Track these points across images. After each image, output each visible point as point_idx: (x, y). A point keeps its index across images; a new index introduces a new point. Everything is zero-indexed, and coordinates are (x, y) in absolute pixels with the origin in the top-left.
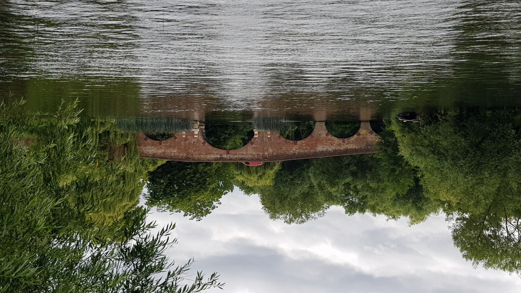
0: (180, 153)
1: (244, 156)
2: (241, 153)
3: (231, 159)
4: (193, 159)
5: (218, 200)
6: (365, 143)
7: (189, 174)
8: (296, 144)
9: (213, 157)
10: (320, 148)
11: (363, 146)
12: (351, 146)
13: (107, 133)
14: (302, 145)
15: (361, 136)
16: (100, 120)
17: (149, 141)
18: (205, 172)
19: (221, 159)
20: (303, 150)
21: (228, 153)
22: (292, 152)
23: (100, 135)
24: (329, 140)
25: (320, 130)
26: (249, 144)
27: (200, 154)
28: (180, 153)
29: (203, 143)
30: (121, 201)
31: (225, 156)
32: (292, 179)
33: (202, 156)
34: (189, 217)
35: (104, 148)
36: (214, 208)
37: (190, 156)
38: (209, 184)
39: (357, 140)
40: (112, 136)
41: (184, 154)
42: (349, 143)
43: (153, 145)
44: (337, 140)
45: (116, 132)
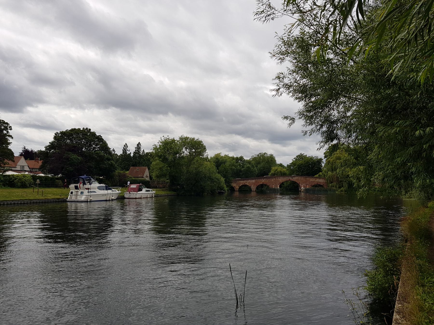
2: (285, 179)
3: (288, 177)
5: (293, 161)
7: (305, 171)
10: (254, 181)
11: (238, 182)
12: (242, 182)
13: (340, 187)
16: (343, 192)
17: (322, 184)
18: (299, 172)
19: (292, 177)
21: (290, 179)
23: (343, 187)
24: (250, 184)
25: (254, 188)
27: (301, 179)
29: (300, 183)
30: (333, 161)
31: (291, 178)
32: (264, 169)
33: (300, 178)
34: (305, 155)
35: (341, 181)
36: (295, 158)
37: (305, 178)
38: (297, 167)
39: (240, 184)
40: (338, 186)
42: (243, 183)
43: (320, 183)
44: (247, 184)
45: (336, 188)
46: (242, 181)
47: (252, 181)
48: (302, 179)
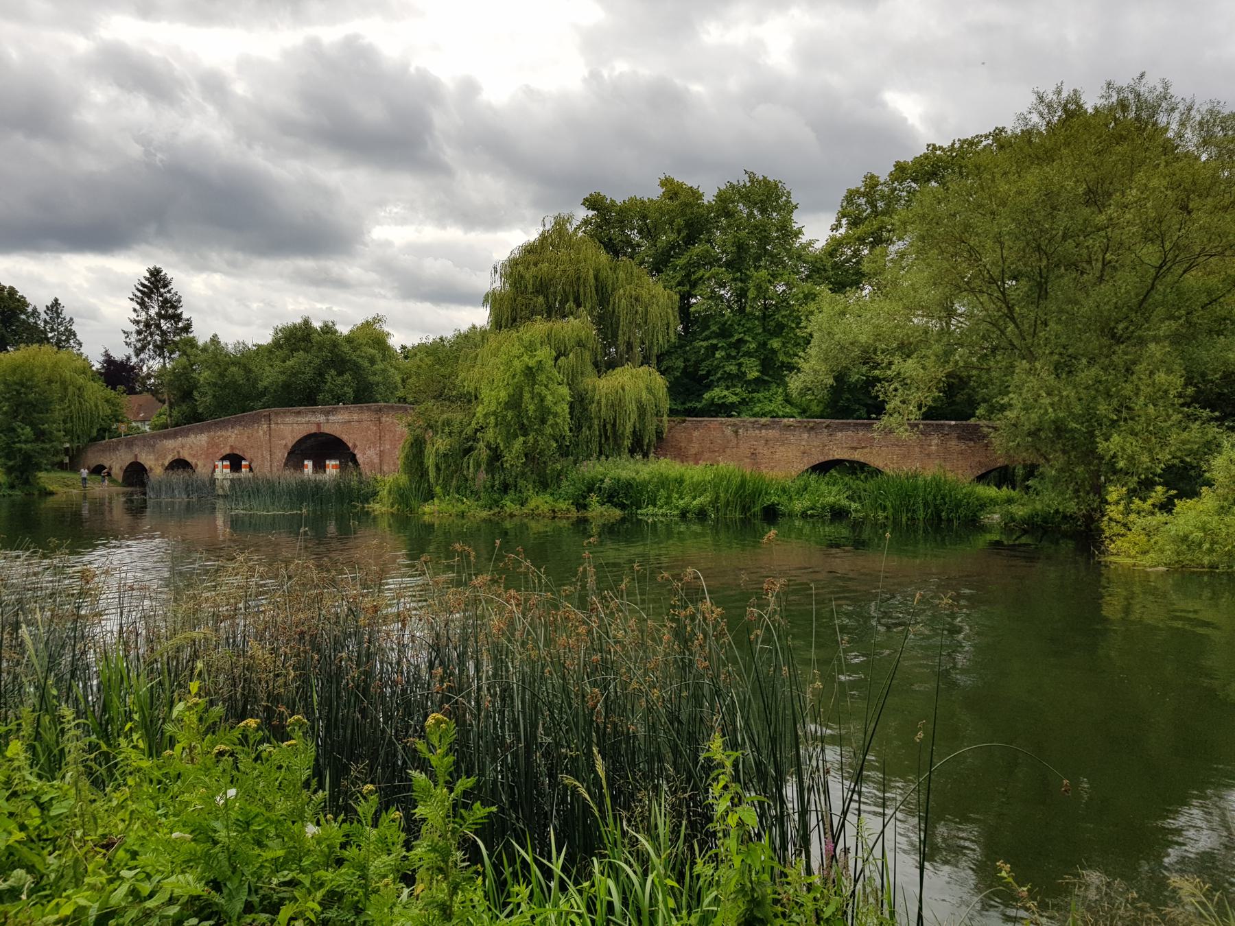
2: (301, 427)
4: (369, 409)
8: (231, 446)
12: (170, 444)
14: (225, 445)
19: (327, 413)
21: (319, 425)
24: (194, 456)
26: (290, 445)
27: (359, 422)
31: (322, 419)
33: (356, 417)
46: (170, 439)
47: (199, 437)
48: (365, 425)
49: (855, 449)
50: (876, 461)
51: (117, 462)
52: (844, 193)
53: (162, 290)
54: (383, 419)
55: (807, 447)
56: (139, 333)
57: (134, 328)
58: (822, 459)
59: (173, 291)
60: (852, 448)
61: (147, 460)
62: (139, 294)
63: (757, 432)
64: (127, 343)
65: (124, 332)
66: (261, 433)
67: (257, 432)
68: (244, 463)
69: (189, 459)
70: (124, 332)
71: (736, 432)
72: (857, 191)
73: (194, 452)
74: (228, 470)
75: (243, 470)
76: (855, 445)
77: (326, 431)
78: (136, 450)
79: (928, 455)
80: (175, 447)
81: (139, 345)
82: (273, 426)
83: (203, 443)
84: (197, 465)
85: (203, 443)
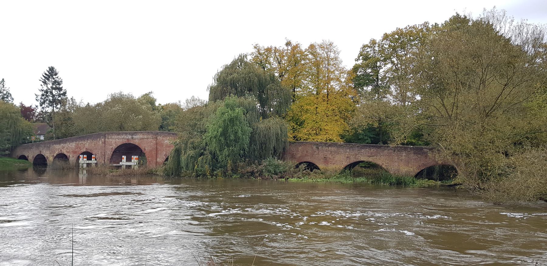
0: (163, 140)
1: (118, 137)
3: (126, 134)
6: (50, 149)
9: (138, 136)
14: (83, 148)
15: (52, 155)
20: (83, 143)
21: (128, 139)
22: (89, 142)
26: (114, 148)
28: (163, 140)
31: (130, 137)
33: (146, 137)
39: (54, 152)
41: (160, 139)
47: (71, 144)
48: (150, 140)
49: (370, 156)
50: (379, 162)
51: (31, 154)
52: (362, 46)
53: (54, 77)
54: (158, 138)
55: (349, 155)
56: (43, 95)
57: (40, 93)
58: (355, 160)
59: (59, 77)
60: (368, 156)
61: (47, 153)
62: (44, 78)
63: (327, 148)
64: (36, 100)
65: (36, 95)
66: (101, 142)
67: (99, 142)
68: (93, 156)
69: (66, 153)
70: (36, 95)
71: (318, 148)
72: (367, 46)
73: (68, 150)
74: (86, 159)
75: (93, 159)
76: (370, 155)
77: (132, 143)
78: (41, 149)
79: (401, 160)
80: (59, 148)
81: (42, 101)
82: (106, 140)
83: (73, 146)
84: (69, 156)
85: (73, 146)
